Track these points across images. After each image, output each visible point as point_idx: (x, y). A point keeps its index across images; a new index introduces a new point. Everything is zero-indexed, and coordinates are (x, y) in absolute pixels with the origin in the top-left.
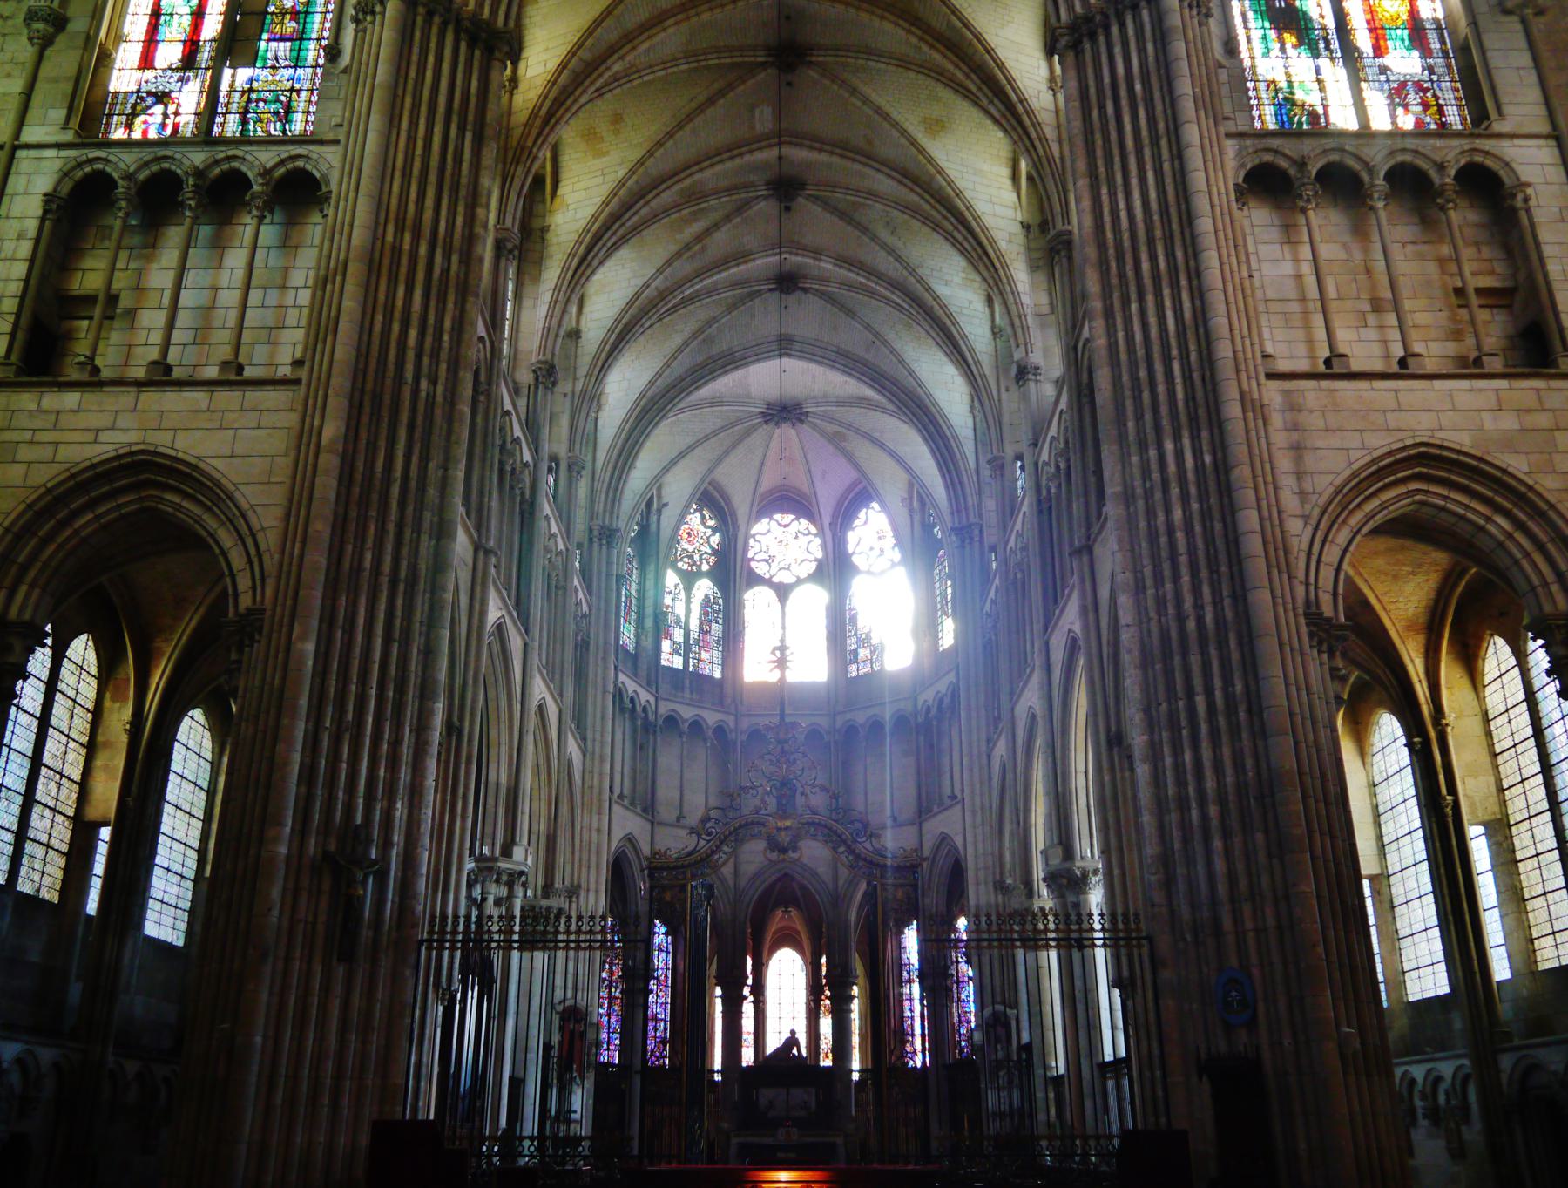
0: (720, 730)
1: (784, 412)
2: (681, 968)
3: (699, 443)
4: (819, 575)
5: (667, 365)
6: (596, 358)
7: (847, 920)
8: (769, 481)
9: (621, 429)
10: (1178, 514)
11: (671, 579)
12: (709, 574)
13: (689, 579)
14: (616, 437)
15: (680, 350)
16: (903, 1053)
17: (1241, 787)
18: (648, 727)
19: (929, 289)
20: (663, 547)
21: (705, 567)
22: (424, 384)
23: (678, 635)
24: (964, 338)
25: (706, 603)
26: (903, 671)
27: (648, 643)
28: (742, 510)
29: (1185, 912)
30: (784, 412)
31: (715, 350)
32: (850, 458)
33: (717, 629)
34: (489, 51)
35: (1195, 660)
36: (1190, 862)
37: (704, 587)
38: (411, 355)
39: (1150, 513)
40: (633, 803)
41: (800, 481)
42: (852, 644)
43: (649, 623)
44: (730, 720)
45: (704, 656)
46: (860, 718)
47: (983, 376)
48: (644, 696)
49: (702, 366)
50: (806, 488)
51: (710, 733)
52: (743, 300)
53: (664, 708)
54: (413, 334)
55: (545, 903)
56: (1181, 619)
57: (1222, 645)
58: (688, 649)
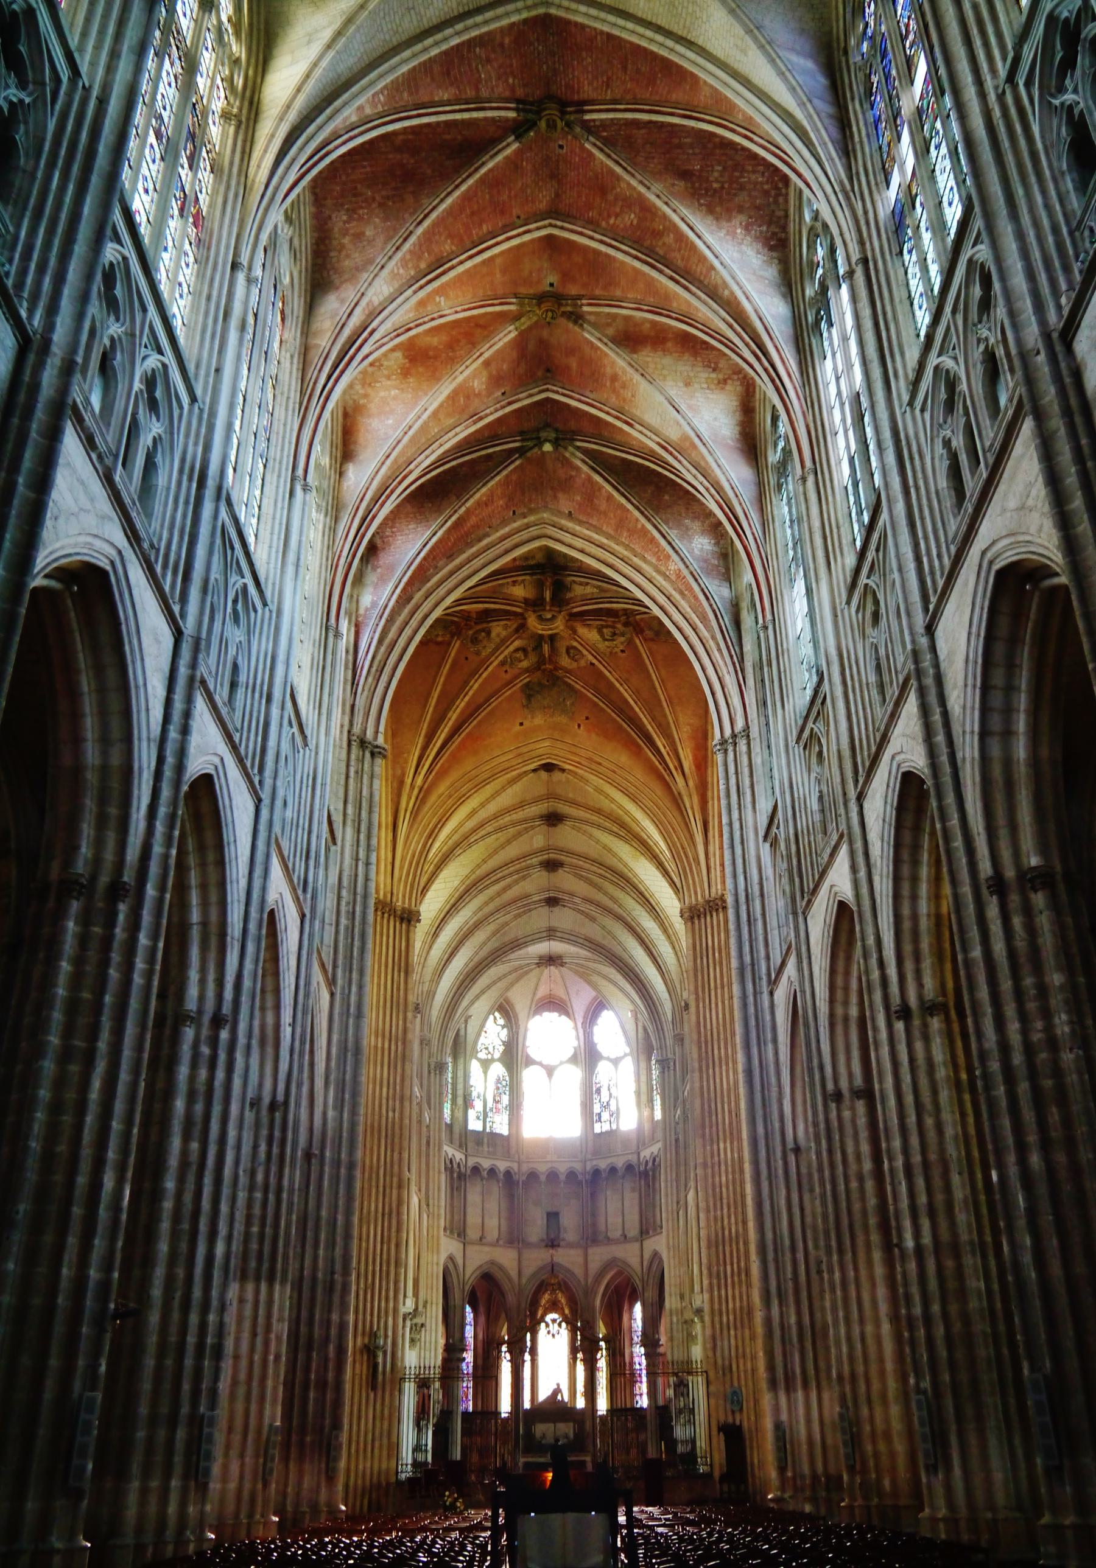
0: (508, 1174)
1: (551, 960)
2: (480, 1336)
3: (494, 983)
4: (574, 1059)
5: (476, 953)
6: (436, 969)
7: (594, 1308)
8: (542, 991)
9: (447, 996)
10: (724, 1179)
11: (475, 1067)
12: (500, 1060)
13: (486, 1064)
14: (445, 1001)
15: (484, 943)
16: (633, 1395)
17: (741, 1308)
18: (462, 1177)
19: (639, 924)
20: (469, 1048)
21: (497, 1055)
22: (391, 1114)
23: (478, 1105)
24: (660, 955)
25: (498, 1081)
26: (630, 1131)
27: (459, 1114)
28: (522, 1016)
29: (720, 1362)
30: (551, 960)
31: (507, 939)
32: (594, 986)
33: (505, 1099)
34: (409, 921)
35: (727, 1249)
36: (722, 1340)
37: (498, 1070)
38: (384, 1101)
39: (713, 1176)
40: (452, 1232)
41: (561, 993)
42: (597, 1109)
43: (460, 1101)
44: (515, 1166)
45: (497, 1118)
46: (603, 1165)
47: (672, 980)
48: (459, 1156)
49: (498, 950)
50: (564, 996)
51: (501, 1176)
52: (525, 913)
53: (471, 1162)
54: (385, 1090)
55: (415, 1321)
56: (723, 1229)
57: (737, 1244)
58: (485, 1115)
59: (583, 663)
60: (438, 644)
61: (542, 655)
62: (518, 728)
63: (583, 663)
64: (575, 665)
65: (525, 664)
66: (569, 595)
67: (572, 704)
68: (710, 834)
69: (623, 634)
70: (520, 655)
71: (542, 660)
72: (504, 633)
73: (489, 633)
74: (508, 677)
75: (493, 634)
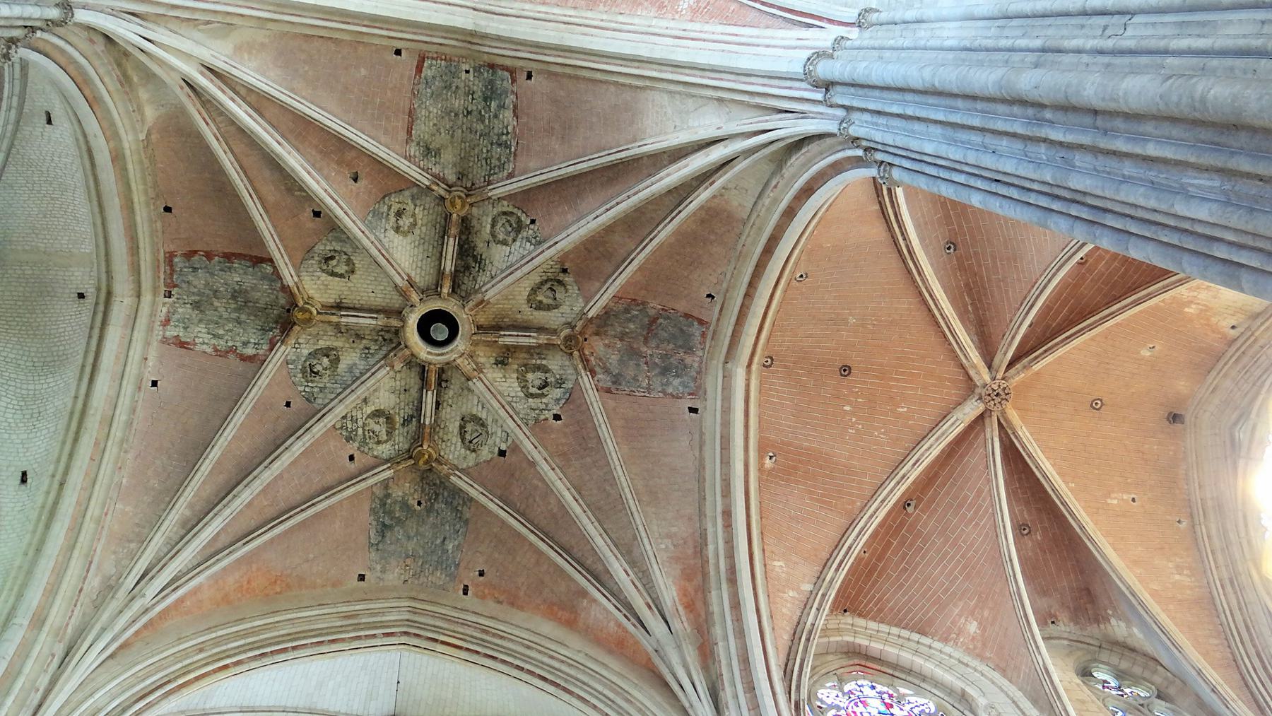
59: (485, 454)
60: (244, 358)
61: (421, 426)
62: (355, 583)
63: (485, 454)
64: (472, 459)
65: (385, 450)
66: (483, 278)
67: (458, 548)
68: (727, 695)
69: (560, 383)
70: (380, 428)
71: (417, 439)
72: (362, 365)
73: (335, 362)
74: (352, 467)
75: (342, 366)
